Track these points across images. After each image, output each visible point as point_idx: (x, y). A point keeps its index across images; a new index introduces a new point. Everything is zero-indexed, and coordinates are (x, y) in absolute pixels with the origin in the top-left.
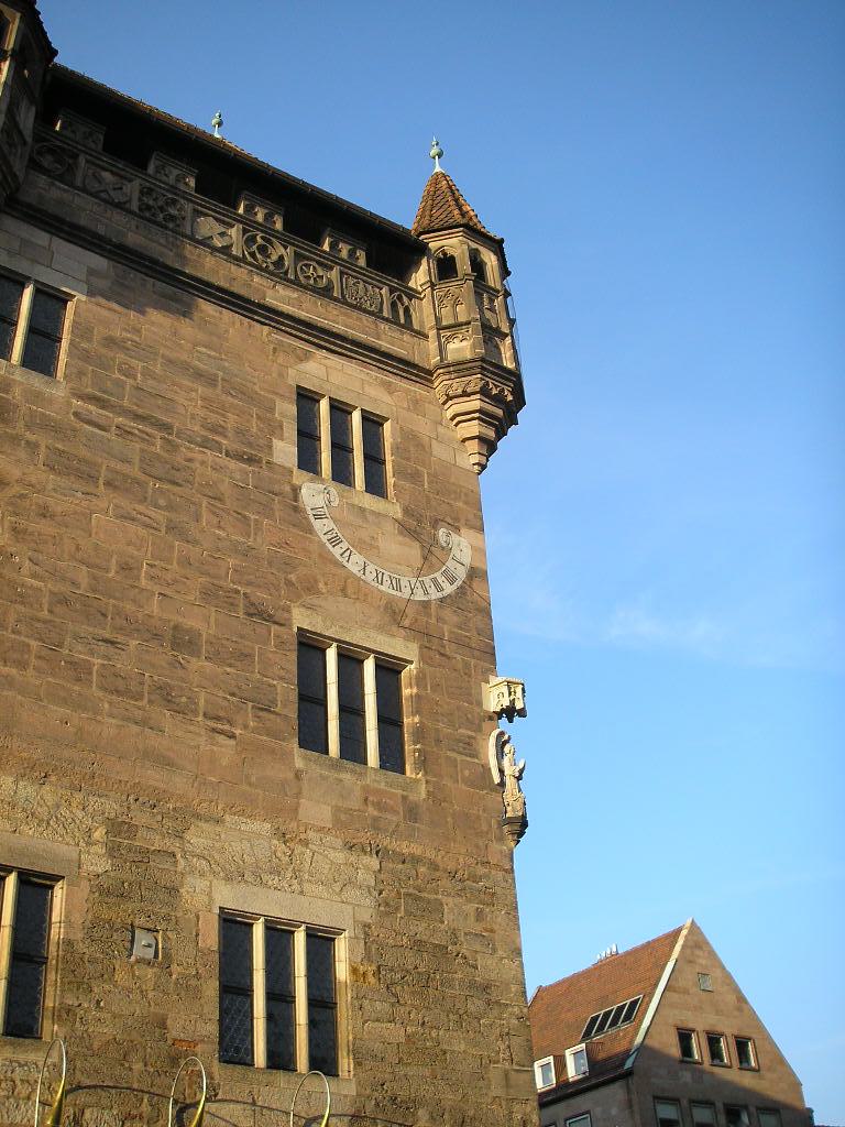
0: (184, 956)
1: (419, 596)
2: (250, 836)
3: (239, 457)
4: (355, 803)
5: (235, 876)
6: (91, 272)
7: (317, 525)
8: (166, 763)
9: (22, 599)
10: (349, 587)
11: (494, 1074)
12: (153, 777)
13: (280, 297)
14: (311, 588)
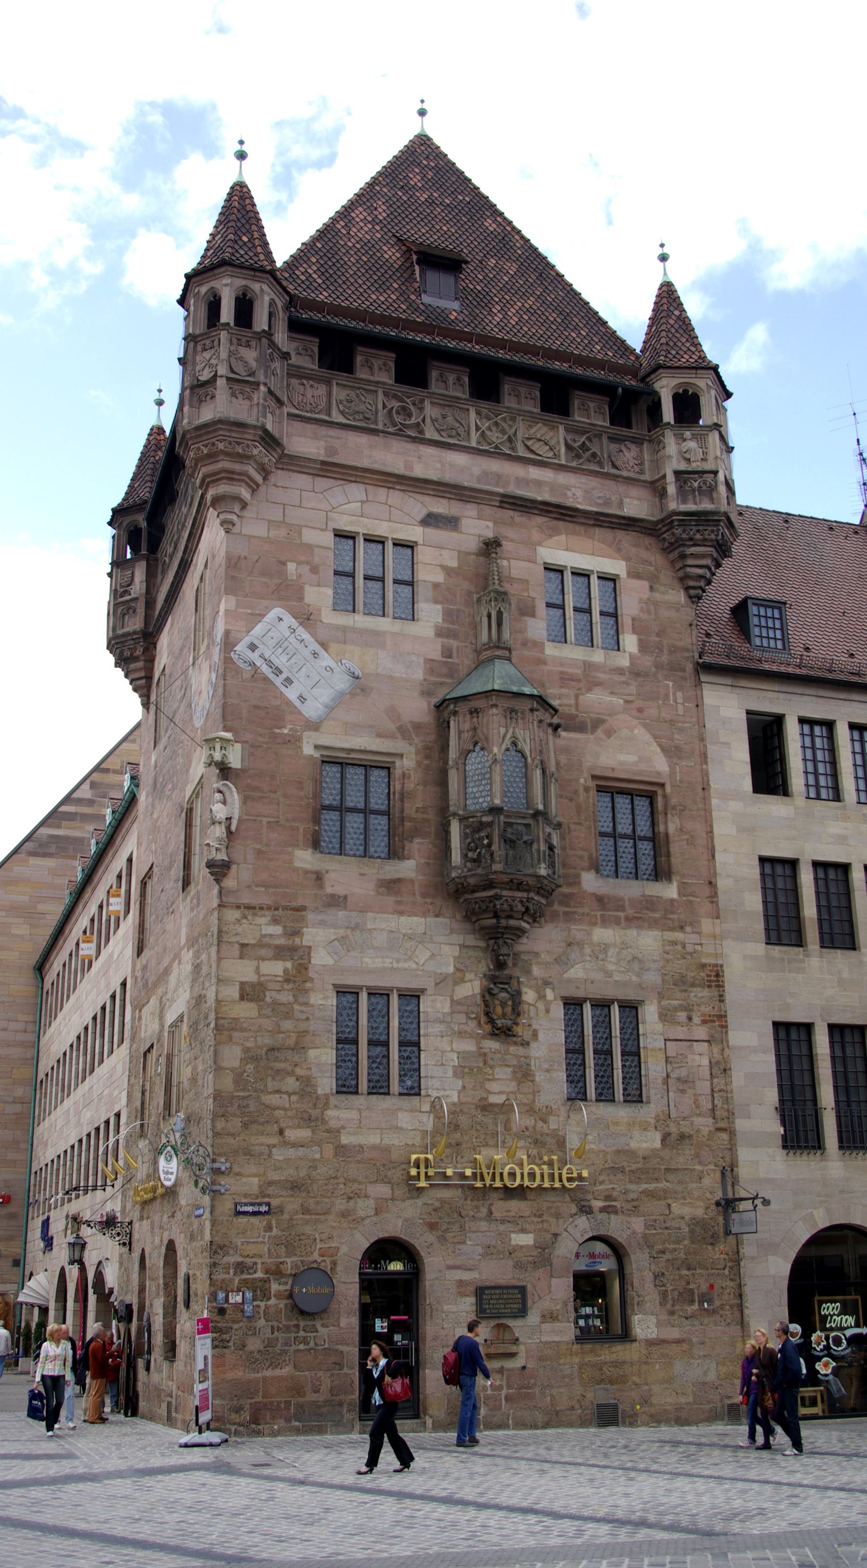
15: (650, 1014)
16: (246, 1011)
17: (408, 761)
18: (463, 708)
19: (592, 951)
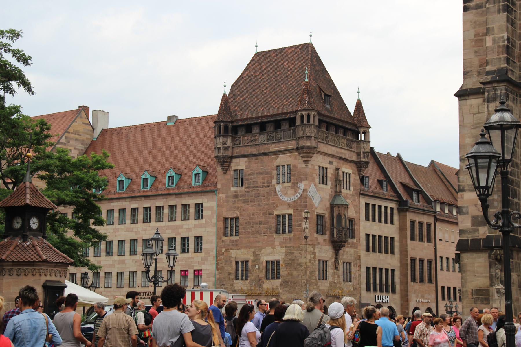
0: (261, 267)
1: (294, 200)
2: (269, 249)
3: (267, 187)
4: (282, 240)
5: (268, 255)
6: (245, 162)
7: (278, 194)
8: (259, 242)
9: (242, 225)
10: (283, 203)
11: (300, 277)
12: (258, 244)
13: (273, 148)
14: (277, 206)
15: (352, 265)
16: (309, 264)
17: (327, 216)
18: (337, 206)
19: (347, 253)
